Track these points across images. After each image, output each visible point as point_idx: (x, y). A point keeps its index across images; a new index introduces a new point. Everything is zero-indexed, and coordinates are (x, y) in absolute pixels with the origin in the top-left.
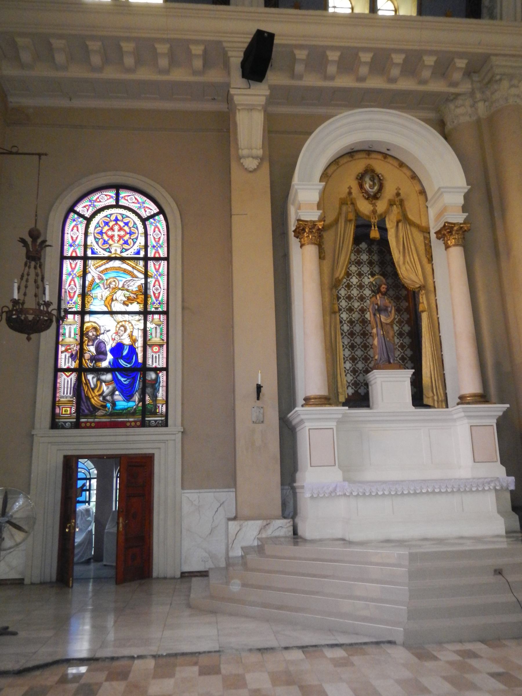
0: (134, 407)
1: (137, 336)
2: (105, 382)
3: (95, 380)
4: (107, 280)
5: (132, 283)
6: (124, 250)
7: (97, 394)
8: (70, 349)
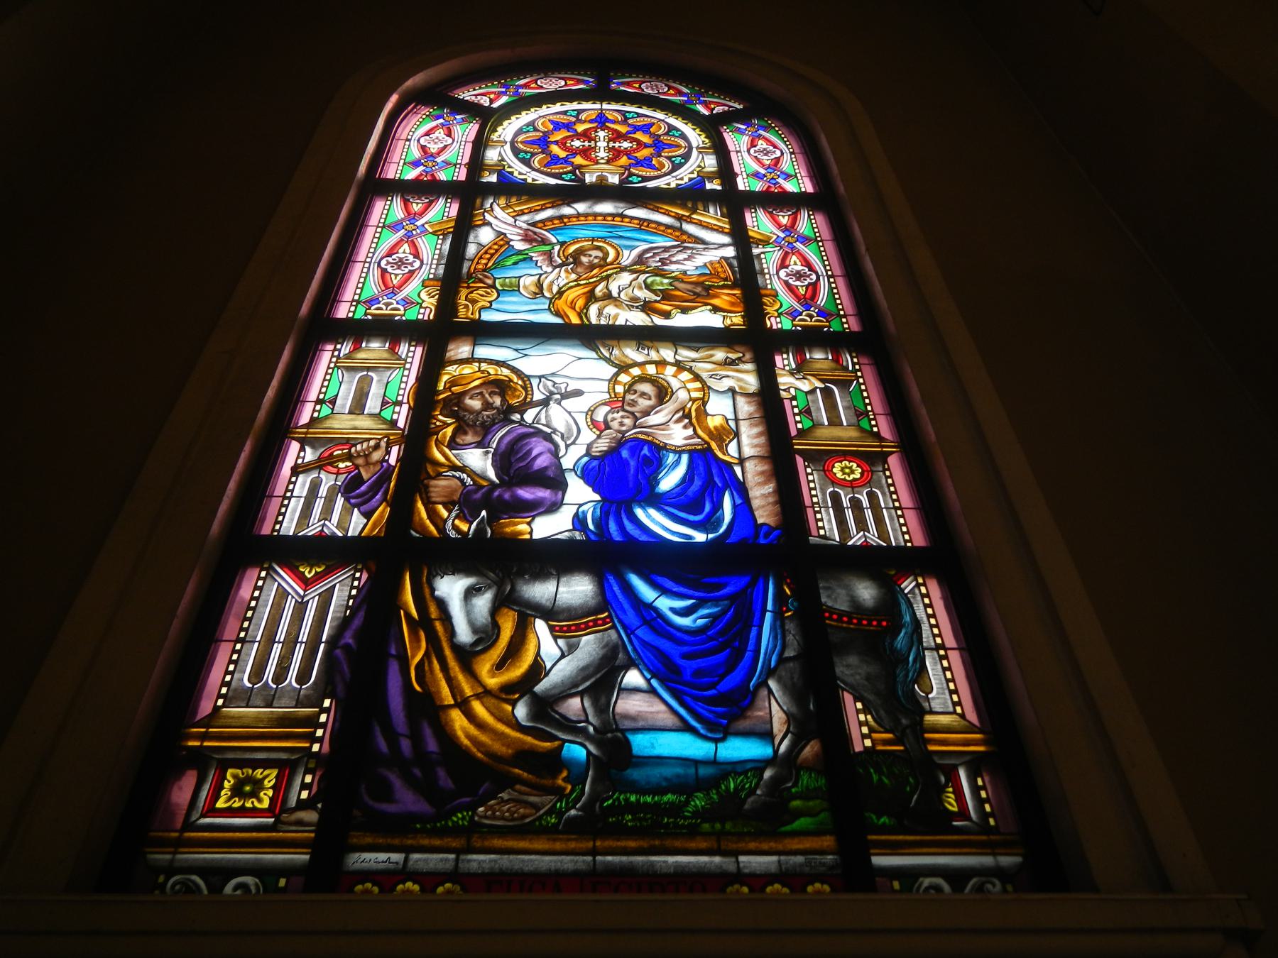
0: (768, 774)
1: (730, 416)
2: (550, 613)
3: (483, 603)
4: (563, 244)
5: (681, 256)
6: (634, 179)
7: (492, 682)
8: (349, 457)
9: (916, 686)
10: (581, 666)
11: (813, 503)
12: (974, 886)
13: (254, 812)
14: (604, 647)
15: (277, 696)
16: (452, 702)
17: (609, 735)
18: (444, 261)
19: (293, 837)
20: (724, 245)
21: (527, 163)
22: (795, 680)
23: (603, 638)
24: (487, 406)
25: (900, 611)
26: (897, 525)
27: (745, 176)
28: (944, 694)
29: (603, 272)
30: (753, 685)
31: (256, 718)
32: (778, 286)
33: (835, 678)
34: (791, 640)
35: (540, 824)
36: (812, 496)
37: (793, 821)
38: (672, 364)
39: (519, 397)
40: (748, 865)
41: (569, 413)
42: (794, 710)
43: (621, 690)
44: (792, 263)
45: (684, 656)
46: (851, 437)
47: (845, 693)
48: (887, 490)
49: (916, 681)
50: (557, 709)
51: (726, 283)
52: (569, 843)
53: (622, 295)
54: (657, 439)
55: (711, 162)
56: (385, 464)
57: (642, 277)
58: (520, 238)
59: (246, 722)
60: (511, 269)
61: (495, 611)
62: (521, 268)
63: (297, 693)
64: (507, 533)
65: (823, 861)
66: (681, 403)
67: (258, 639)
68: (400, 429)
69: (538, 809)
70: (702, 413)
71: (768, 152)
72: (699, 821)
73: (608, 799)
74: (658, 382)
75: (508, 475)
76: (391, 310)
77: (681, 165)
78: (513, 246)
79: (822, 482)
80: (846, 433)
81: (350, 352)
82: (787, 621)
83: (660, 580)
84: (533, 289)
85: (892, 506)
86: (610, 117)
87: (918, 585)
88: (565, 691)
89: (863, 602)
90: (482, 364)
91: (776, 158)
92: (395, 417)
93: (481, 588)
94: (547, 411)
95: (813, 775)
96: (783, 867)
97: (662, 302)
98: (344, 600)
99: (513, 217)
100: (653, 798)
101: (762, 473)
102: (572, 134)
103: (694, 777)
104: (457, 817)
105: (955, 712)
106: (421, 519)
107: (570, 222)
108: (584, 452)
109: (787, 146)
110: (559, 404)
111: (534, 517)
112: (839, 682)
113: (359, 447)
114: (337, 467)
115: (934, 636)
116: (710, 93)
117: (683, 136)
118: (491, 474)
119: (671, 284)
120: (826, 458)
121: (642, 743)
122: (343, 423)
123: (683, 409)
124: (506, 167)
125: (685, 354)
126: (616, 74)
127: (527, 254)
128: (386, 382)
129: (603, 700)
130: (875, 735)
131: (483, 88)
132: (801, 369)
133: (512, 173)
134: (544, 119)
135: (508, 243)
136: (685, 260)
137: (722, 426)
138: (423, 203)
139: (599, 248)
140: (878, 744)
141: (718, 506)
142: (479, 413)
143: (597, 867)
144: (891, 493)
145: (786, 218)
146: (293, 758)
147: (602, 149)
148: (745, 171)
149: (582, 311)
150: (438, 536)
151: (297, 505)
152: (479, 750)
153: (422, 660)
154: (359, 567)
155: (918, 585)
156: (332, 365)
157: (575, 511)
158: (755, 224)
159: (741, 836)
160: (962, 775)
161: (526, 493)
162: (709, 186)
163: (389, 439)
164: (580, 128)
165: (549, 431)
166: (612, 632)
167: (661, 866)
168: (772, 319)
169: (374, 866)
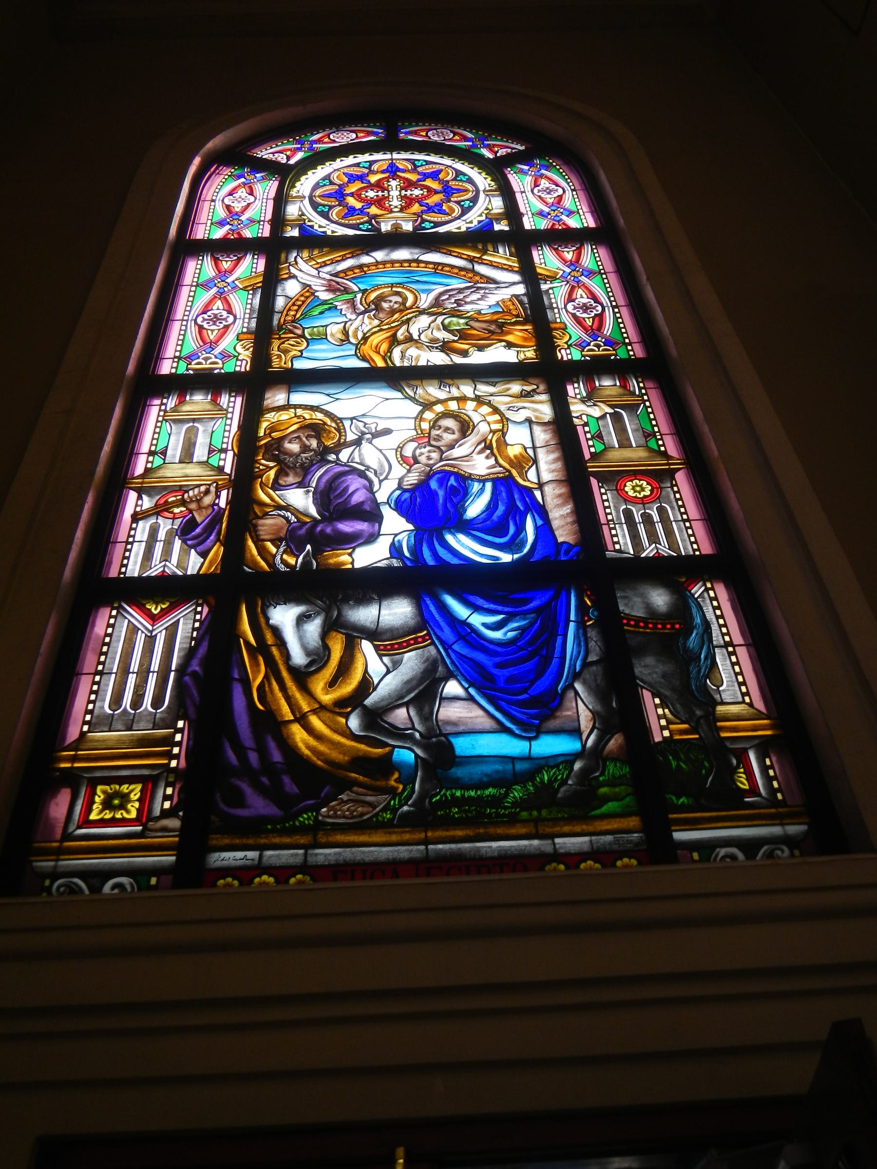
0: (577, 766)
1: (529, 444)
2: (374, 634)
3: (313, 628)
4: (364, 291)
5: (475, 297)
7: (327, 698)
8: (183, 503)
9: (708, 681)
10: (405, 680)
11: (608, 521)
12: (764, 853)
13: (124, 822)
14: (424, 662)
15: (135, 720)
16: (292, 718)
17: (434, 740)
18: (255, 315)
19: (159, 841)
20: (514, 284)
21: (325, 215)
22: (599, 681)
23: (423, 654)
24: (305, 448)
25: (691, 614)
26: (686, 535)
27: (530, 215)
28: (734, 686)
29: (403, 317)
30: (561, 688)
31: (119, 740)
32: (567, 319)
33: (635, 677)
34: (593, 647)
35: (377, 819)
36: (607, 514)
37: (600, 807)
38: (472, 400)
39: (333, 438)
40: (564, 846)
41: (380, 451)
42: (598, 708)
43: (442, 699)
44: (579, 296)
45: (496, 666)
46: (640, 458)
47: (644, 691)
48: (675, 504)
49: (707, 676)
50: (385, 719)
51: (518, 319)
52: (404, 835)
53: (423, 337)
54: (462, 470)
55: (497, 204)
56: (216, 507)
57: (440, 319)
58: (324, 288)
59: (110, 744)
60: (318, 318)
61: (324, 635)
62: (327, 317)
63: (153, 717)
64: (331, 564)
65: (630, 838)
66: (483, 436)
67: (115, 670)
68: (228, 475)
69: (375, 807)
70: (503, 443)
71: (551, 191)
72: (518, 810)
73: (436, 795)
74: (460, 417)
75: (328, 510)
76: (211, 363)
77: (470, 209)
78: (318, 297)
79: (615, 501)
80: (636, 454)
81: (175, 406)
82: (589, 629)
83: (472, 598)
84: (340, 336)
85: (680, 518)
86: (400, 167)
87: (707, 590)
88: (392, 703)
89: (657, 608)
90: (298, 410)
91: (558, 196)
92: (222, 463)
93: (311, 615)
94: (359, 451)
95: (618, 765)
96: (595, 846)
97: (460, 341)
98: (188, 633)
99: (316, 269)
100: (476, 793)
101: (560, 495)
102: (366, 185)
103: (512, 772)
104: (303, 817)
105: (743, 702)
106: (252, 555)
107: (370, 270)
108: (396, 486)
109: (568, 184)
110: (371, 443)
111: (354, 548)
112: (638, 681)
113: (191, 493)
114: (172, 512)
115: (723, 635)
116: (493, 136)
117: (470, 181)
118: (313, 511)
119: (467, 324)
120: (618, 478)
121: (463, 746)
122: (174, 472)
123: (485, 440)
124: (307, 221)
125: (484, 389)
126: (403, 124)
127: (332, 303)
128: (211, 431)
129: (427, 709)
130: (671, 727)
131: (280, 146)
132: (590, 398)
133: (312, 227)
134: (339, 172)
135: (313, 294)
136: (479, 299)
137: (521, 454)
138: (232, 261)
139: (398, 294)
140: (676, 734)
141: (521, 528)
142: (298, 455)
143: (430, 854)
144: (679, 507)
145: (571, 253)
146: (154, 773)
147: (395, 198)
148: (530, 211)
149: (386, 354)
150: (269, 570)
151: (139, 549)
152: (318, 759)
153: (262, 681)
154: (200, 602)
155: (707, 590)
156: (160, 419)
157: (392, 541)
158: (542, 261)
159: (555, 821)
160: (752, 756)
161: (346, 527)
162: (497, 227)
163: (217, 484)
164: (373, 179)
165: (363, 468)
166: (432, 648)
167: (486, 850)
168: (563, 351)
169: (234, 863)
